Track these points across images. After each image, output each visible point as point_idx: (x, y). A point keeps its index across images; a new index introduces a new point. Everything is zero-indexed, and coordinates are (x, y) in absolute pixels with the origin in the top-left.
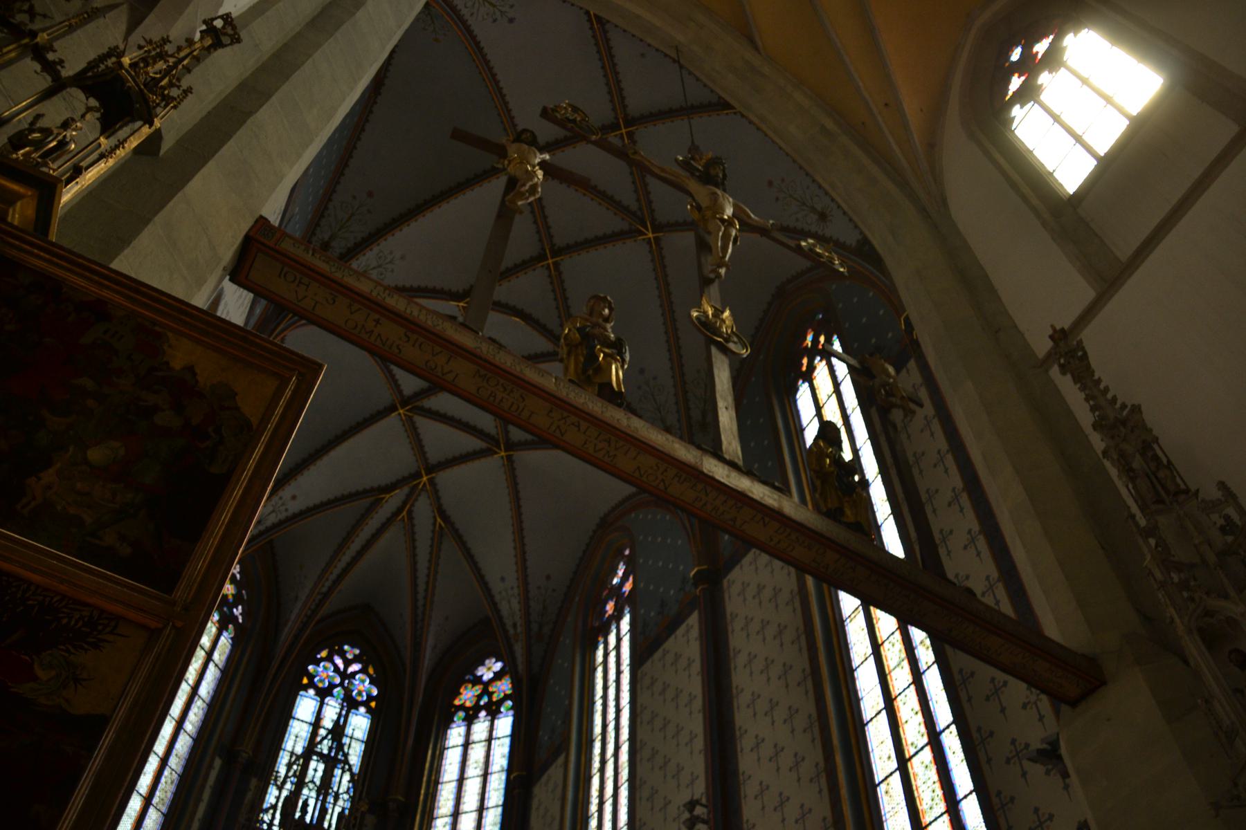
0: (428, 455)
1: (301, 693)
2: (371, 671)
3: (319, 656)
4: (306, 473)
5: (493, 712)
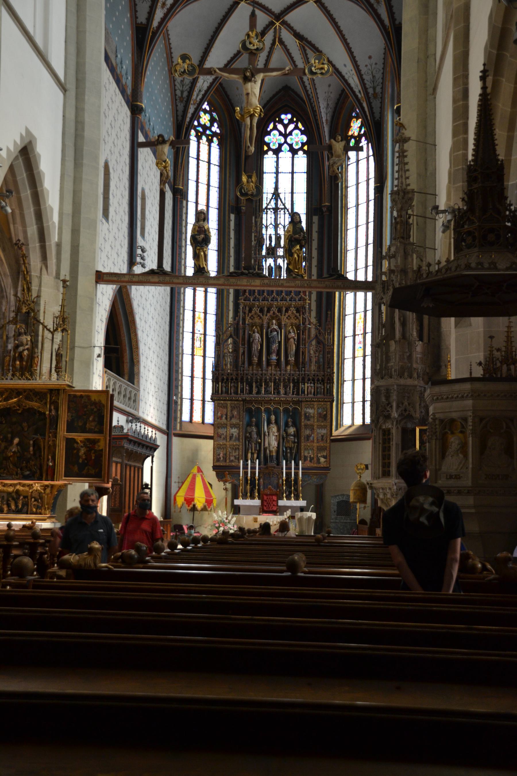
0: (273, 10)
1: (266, 156)
2: (300, 125)
3: (269, 130)
4: (210, 54)
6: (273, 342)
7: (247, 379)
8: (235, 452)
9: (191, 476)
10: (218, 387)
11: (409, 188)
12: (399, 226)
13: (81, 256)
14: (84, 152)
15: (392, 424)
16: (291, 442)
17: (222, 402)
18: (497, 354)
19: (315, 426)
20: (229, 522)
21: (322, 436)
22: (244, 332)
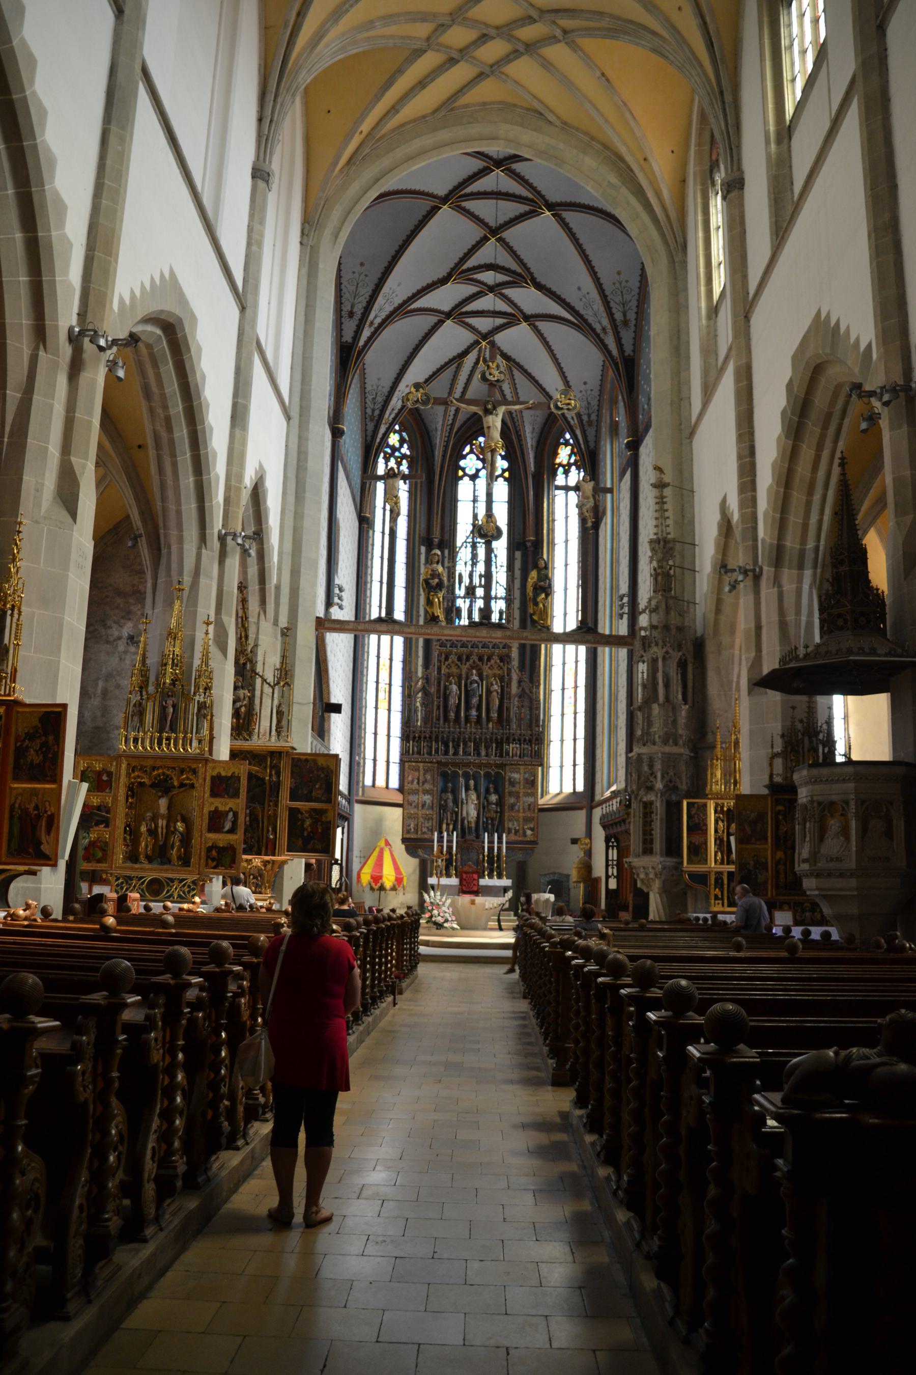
1: (460, 482)
3: (464, 453)
7: (443, 737)
9: (377, 850)
11: (669, 536)
12: (660, 578)
13: (301, 600)
14: (307, 485)
15: (656, 796)
18: (799, 726)
19: (521, 794)
20: (443, 904)
21: (529, 805)
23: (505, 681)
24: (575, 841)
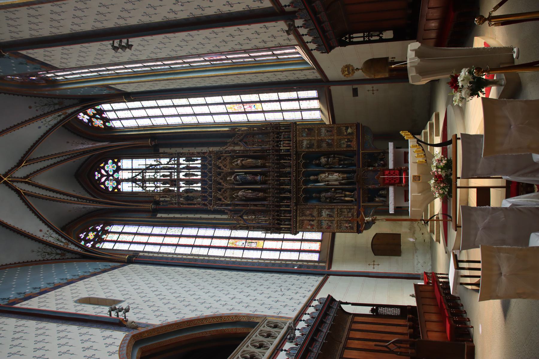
2: (102, 165)
5: (101, 112)
6: (246, 179)
7: (277, 202)
8: (344, 212)
10: (285, 228)
16: (334, 161)
17: (298, 224)
21: (328, 131)
22: (237, 205)
23: (235, 156)
24: (355, 92)
